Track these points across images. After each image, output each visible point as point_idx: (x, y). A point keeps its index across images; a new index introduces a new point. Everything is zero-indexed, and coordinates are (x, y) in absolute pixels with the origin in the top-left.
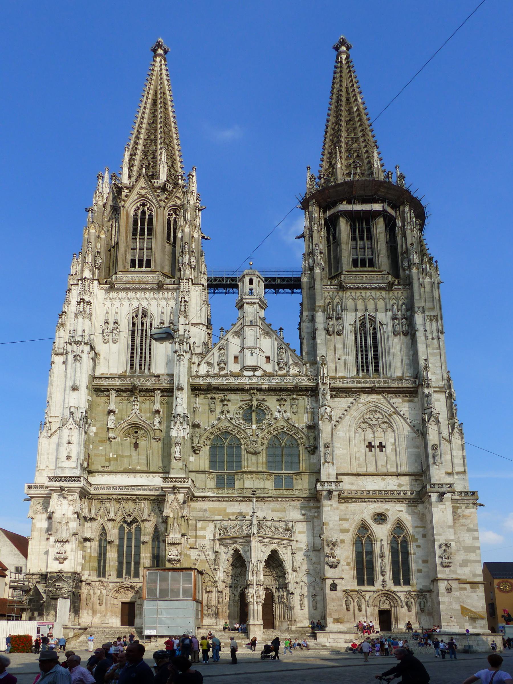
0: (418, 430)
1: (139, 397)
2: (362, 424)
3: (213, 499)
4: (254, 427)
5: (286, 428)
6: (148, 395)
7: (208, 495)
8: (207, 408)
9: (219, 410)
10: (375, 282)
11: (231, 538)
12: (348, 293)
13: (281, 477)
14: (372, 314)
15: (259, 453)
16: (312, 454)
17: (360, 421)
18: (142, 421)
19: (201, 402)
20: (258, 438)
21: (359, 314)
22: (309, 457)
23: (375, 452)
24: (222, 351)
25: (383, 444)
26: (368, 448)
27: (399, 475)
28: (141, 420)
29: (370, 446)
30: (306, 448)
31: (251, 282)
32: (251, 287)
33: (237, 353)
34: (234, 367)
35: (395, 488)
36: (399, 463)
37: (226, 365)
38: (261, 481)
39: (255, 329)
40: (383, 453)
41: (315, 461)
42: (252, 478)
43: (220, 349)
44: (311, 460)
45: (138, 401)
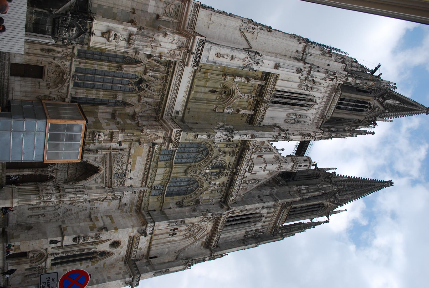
1: (253, 99)
9: (227, 149)
11: (111, 167)
15: (185, 174)
18: (234, 100)
20: (198, 174)
23: (169, 233)
24: (268, 150)
25: (174, 236)
27: (149, 248)
28: (235, 99)
30: (182, 200)
33: (263, 157)
35: (139, 247)
36: (159, 245)
38: (162, 178)
45: (250, 98)
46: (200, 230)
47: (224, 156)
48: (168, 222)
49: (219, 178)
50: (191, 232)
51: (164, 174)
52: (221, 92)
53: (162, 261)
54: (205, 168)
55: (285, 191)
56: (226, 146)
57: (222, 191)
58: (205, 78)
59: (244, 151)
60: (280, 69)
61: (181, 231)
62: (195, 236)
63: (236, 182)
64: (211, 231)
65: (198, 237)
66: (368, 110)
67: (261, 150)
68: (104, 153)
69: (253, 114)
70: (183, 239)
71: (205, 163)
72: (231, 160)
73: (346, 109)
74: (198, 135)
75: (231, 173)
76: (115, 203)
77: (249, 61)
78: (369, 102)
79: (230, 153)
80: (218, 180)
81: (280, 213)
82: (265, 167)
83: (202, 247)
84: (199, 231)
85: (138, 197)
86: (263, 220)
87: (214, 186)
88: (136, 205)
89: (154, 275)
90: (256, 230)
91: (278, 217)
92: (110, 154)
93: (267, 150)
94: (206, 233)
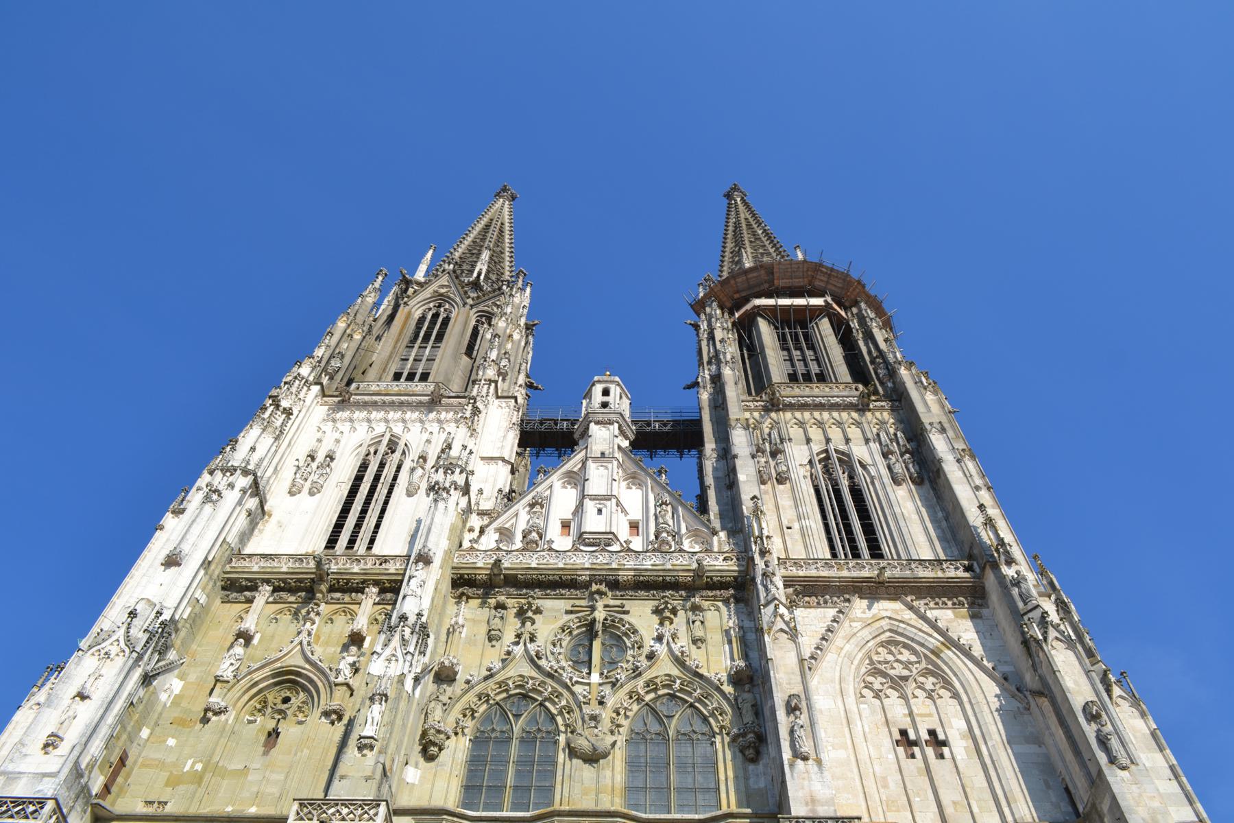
1: (323, 606)
2: (870, 679)
4: (595, 678)
5: (678, 682)
6: (347, 598)
8: (483, 630)
17: (863, 670)
19: (469, 616)
22: (745, 770)
25: (941, 737)
28: (307, 660)
31: (606, 392)
32: (606, 399)
39: (610, 465)
40: (947, 763)
41: (762, 785)
44: (752, 781)
45: (318, 614)
46: (897, 643)
47: (532, 639)
48: (792, 765)
49: (635, 632)
50: (914, 674)
52: (281, 712)
53: (1069, 756)
54: (578, 689)
56: (494, 643)
57: (696, 608)
58: (198, 778)
60: (186, 548)
61: (911, 714)
62: (933, 652)
63: (646, 570)
65: (934, 641)
66: (445, 310)
67: (531, 532)
69: (375, 590)
70: (956, 696)
71: (559, 695)
72: (558, 611)
73: (431, 360)
74: (361, 737)
75: (615, 598)
77: (118, 640)
78: (417, 314)
79: (523, 624)
80: (642, 631)
81: (803, 407)
82: (594, 498)
83: (985, 612)
86: (843, 447)
87: (665, 641)
89: (1124, 768)
91: (820, 407)
94: (908, 615)
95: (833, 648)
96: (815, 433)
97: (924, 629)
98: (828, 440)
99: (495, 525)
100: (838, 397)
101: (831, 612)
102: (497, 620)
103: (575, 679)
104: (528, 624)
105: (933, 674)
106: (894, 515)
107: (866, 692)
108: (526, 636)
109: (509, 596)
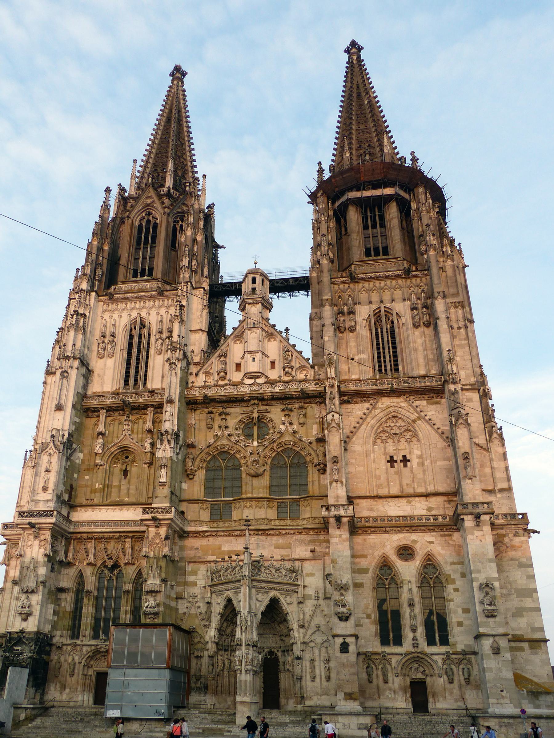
0: (447, 438)
2: (382, 435)
3: (206, 534)
7: (200, 529)
9: (216, 427)
10: (389, 270)
12: (361, 285)
13: (286, 504)
14: (388, 305)
16: (322, 474)
17: (379, 431)
21: (374, 307)
22: (319, 477)
24: (222, 359)
26: (389, 464)
29: (392, 461)
30: (315, 466)
34: (236, 377)
37: (226, 374)
38: (262, 509)
42: (251, 506)
43: (221, 357)
44: (322, 482)
46: (397, 417)
47: (226, 427)
51: (254, 507)
55: (317, 292)
57: (302, 408)
59: (215, 399)
62: (412, 421)
64: (398, 396)
67: (220, 372)
68: (209, 595)
76: (308, 567)
80: (276, 421)
84: (400, 418)
85: (299, 536)
88: (316, 536)
90: (413, 308)
92: (210, 586)
93: (221, 361)
95: (365, 423)
96: (375, 297)
97: (410, 411)
98: (382, 302)
99: (202, 371)
100: (390, 271)
101: (367, 405)
102: (209, 420)
103: (247, 445)
104: (224, 421)
105: (410, 431)
106: (410, 348)
107: (379, 441)
108: (223, 427)
109: (214, 407)
